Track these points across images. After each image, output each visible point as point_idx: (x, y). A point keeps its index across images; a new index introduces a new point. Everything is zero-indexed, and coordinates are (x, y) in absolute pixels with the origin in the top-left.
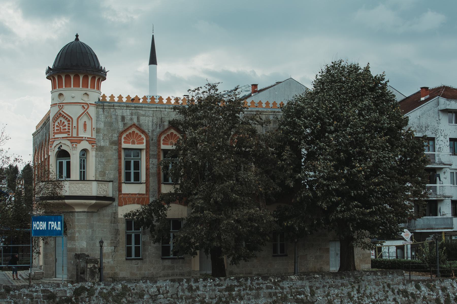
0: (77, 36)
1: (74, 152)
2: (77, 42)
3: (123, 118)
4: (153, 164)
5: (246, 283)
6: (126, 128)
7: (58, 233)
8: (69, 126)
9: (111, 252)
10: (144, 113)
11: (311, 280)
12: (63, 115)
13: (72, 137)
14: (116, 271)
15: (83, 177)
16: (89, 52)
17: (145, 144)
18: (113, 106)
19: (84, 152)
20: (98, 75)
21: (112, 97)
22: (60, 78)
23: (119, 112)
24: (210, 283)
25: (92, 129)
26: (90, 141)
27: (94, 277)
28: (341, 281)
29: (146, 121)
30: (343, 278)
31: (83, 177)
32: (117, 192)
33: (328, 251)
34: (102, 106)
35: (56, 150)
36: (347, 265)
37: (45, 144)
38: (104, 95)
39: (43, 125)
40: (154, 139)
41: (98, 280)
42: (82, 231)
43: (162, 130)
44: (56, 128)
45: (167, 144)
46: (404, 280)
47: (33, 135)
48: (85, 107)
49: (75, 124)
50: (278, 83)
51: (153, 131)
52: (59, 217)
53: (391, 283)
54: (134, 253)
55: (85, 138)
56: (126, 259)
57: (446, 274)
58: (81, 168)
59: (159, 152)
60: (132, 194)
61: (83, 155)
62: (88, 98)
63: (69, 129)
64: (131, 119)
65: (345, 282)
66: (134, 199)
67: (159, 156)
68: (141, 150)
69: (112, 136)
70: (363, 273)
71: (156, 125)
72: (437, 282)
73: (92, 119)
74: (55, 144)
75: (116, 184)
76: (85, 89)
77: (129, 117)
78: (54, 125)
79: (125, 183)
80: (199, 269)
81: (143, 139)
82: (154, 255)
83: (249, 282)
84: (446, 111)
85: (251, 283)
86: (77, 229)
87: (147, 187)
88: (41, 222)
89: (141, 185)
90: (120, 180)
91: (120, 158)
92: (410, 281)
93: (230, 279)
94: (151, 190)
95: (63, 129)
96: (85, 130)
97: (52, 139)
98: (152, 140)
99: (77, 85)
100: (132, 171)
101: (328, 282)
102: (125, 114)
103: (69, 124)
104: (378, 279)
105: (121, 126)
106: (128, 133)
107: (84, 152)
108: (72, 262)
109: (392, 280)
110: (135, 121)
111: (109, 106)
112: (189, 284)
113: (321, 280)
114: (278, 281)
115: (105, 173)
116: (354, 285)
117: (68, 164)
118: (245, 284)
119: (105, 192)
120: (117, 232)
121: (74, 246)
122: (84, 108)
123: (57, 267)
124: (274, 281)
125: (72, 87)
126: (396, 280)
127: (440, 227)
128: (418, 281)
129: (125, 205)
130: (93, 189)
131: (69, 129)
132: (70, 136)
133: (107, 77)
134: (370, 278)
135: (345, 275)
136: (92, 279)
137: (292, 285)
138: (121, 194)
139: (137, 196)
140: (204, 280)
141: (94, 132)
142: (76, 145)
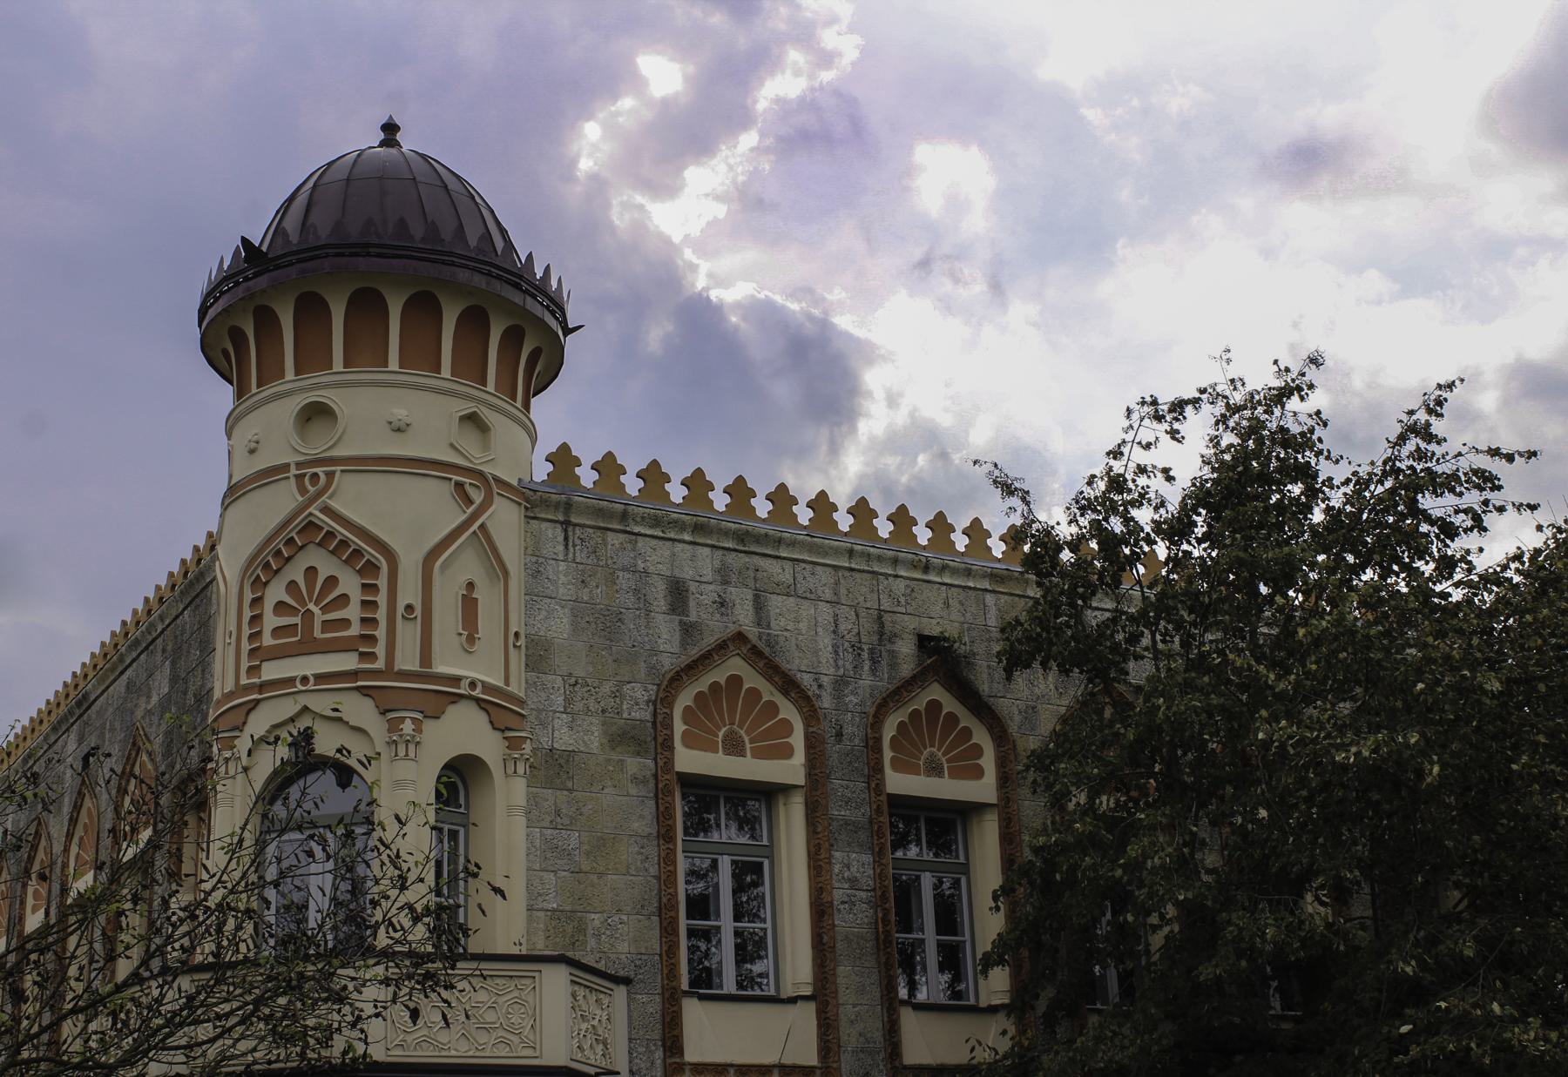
0: (390, 128)
1: (405, 770)
3: (678, 593)
4: (853, 882)
6: (695, 652)
8: (368, 605)
10: (787, 577)
12: (331, 534)
13: (389, 672)
17: (799, 757)
18: (624, 516)
19: (460, 777)
21: (608, 467)
22: (311, 310)
23: (657, 557)
25: (511, 640)
26: (498, 709)
29: (803, 626)
32: (659, 1054)
34: (557, 506)
38: (564, 448)
43: (885, 684)
44: (271, 621)
48: (471, 492)
49: (409, 592)
51: (840, 683)
55: (473, 685)
62: (486, 446)
63: (368, 622)
64: (722, 604)
71: (856, 648)
74: (259, 724)
75: (652, 1004)
77: (710, 593)
78: (257, 601)
79: (702, 998)
81: (787, 727)
89: (790, 1008)
90: (672, 973)
94: (849, 1035)
95: (327, 625)
99: (422, 355)
102: (687, 573)
106: (703, 684)
107: (460, 777)
110: (744, 616)
111: (600, 513)
115: (581, 930)
122: (470, 502)
125: (394, 364)
131: (372, 622)
132: (380, 664)
138: (681, 1067)
141: (517, 660)
142: (418, 730)
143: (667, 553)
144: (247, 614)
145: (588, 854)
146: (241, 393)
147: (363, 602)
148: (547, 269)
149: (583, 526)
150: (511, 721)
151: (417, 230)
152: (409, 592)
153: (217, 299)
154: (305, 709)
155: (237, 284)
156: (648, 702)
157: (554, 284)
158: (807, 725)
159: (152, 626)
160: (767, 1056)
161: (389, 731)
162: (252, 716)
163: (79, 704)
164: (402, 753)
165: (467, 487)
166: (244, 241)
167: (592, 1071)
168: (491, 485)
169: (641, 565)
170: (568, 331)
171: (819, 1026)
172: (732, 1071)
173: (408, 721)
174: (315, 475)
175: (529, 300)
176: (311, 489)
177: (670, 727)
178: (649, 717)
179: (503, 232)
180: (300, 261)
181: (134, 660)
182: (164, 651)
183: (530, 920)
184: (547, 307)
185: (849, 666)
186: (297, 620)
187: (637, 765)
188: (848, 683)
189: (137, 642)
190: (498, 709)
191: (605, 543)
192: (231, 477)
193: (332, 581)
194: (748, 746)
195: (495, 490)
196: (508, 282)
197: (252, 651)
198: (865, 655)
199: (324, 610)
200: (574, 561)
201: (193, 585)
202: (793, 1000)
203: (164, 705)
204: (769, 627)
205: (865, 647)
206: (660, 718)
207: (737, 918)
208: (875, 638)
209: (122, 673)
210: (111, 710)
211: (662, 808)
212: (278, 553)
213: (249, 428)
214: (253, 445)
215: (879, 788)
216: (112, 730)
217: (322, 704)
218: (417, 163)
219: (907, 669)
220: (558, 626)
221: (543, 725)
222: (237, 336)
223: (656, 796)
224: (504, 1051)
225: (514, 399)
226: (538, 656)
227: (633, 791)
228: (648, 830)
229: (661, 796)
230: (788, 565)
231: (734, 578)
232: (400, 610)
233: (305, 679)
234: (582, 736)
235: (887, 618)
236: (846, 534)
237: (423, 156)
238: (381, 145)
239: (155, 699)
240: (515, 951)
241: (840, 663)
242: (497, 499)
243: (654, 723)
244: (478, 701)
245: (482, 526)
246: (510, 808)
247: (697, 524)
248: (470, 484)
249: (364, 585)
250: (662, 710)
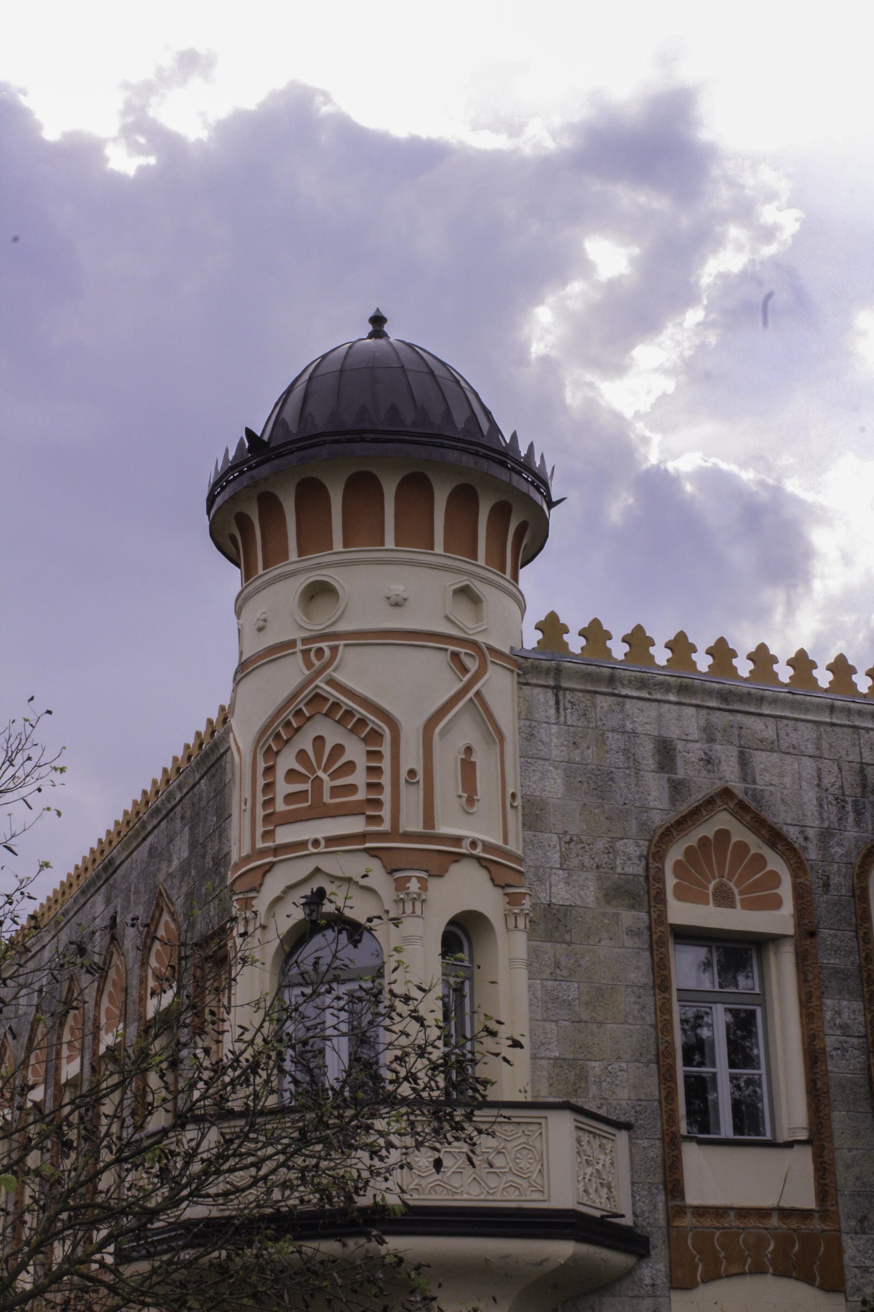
0: (378, 321)
3: (666, 753)
4: (845, 1029)
6: (684, 808)
12: (336, 705)
13: (394, 834)
17: (788, 908)
18: (612, 680)
21: (595, 633)
22: (311, 494)
23: (645, 718)
25: (508, 800)
29: (787, 780)
32: (661, 1198)
34: (548, 671)
35: (293, 914)
38: (553, 617)
40: (835, 880)
44: (283, 788)
48: (467, 661)
49: (411, 758)
51: (826, 835)
55: (474, 844)
60: (744, 1213)
62: (479, 618)
71: (840, 801)
74: (273, 886)
77: (695, 751)
78: (270, 770)
79: (701, 1142)
81: (774, 879)
87: (823, 1170)
89: (788, 1154)
90: (671, 1119)
95: (336, 791)
99: (416, 534)
102: (674, 733)
103: (374, 755)
106: (693, 838)
107: (462, 935)
110: (729, 773)
111: (588, 677)
115: (583, 1076)
122: (465, 670)
125: (390, 542)
129: (713, 1276)
130: (556, 1166)
132: (386, 827)
138: (682, 1210)
139: (774, 1221)
141: (515, 820)
142: (424, 888)
143: (654, 714)
144: (261, 782)
145: (587, 1004)
146: (248, 574)
147: (370, 769)
148: (531, 447)
149: (573, 690)
150: (511, 878)
151: (408, 416)
153: (223, 488)
154: (317, 870)
155: (242, 473)
156: (640, 857)
157: (538, 463)
159: (171, 795)
160: (764, 1198)
161: (397, 889)
162: (269, 879)
163: (105, 869)
164: (409, 910)
165: (463, 657)
166: (249, 433)
167: (598, 1214)
168: (485, 654)
169: (629, 726)
170: (551, 504)
171: (816, 1170)
172: (732, 1214)
173: (414, 880)
174: (320, 651)
175: (515, 477)
176: (317, 663)
177: (661, 880)
178: (640, 870)
179: (488, 413)
180: (299, 449)
181: (155, 827)
182: (183, 818)
183: (534, 1068)
184: (532, 483)
185: (834, 818)
186: (307, 786)
187: (632, 918)
188: (832, 835)
189: (157, 810)
190: (497, 866)
191: (594, 706)
192: (241, 654)
193: (338, 749)
194: (738, 898)
195: (489, 658)
196: (494, 460)
197: (267, 818)
198: (849, 807)
199: (333, 776)
200: (565, 723)
201: (208, 756)
202: (789, 1145)
203: (184, 870)
204: (754, 782)
205: (849, 800)
206: (652, 872)
207: (732, 1064)
208: (858, 790)
209: (144, 839)
210: (134, 873)
211: (656, 959)
212: (288, 724)
213: (257, 608)
214: (261, 623)
216: (137, 892)
217: (332, 865)
218: (404, 351)
220: (553, 786)
221: (541, 880)
222: (243, 522)
223: (651, 948)
224: (513, 1195)
225: (503, 570)
226: (534, 814)
227: (629, 942)
228: (644, 980)
230: (771, 722)
231: (719, 736)
232: (403, 774)
233: (316, 843)
236: (826, 691)
237: (410, 346)
238: (371, 336)
239: (175, 863)
240: (521, 1098)
241: (825, 815)
242: (491, 668)
243: (647, 877)
244: (479, 859)
245: (478, 694)
246: (512, 961)
247: (681, 684)
248: (465, 654)
249: (369, 753)
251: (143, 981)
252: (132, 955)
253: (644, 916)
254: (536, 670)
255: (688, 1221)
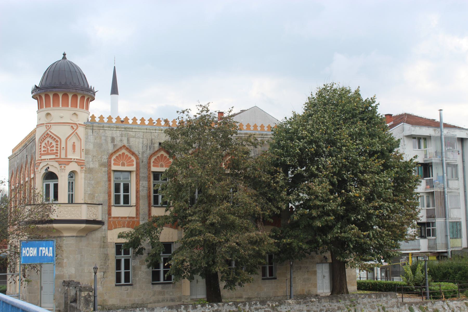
0: (64, 54)
1: (63, 174)
2: (65, 61)
3: (113, 139)
4: (144, 187)
5: (244, 308)
6: (116, 149)
7: (49, 260)
8: (57, 147)
9: (101, 278)
10: (134, 135)
11: (308, 304)
12: (51, 136)
13: (60, 158)
14: (106, 297)
15: (71, 200)
16: (77, 71)
17: (135, 166)
18: (103, 127)
20: (87, 95)
21: (101, 118)
22: (47, 96)
23: (109, 133)
24: (209, 309)
25: (81, 150)
26: (79, 163)
27: (89, 305)
28: (337, 304)
30: (339, 302)
31: (71, 200)
32: (107, 216)
33: (315, 273)
35: (43, 171)
36: (338, 287)
37: (26, 167)
38: (93, 115)
39: (23, 147)
40: (144, 161)
41: (92, 309)
42: (71, 256)
43: (152, 152)
44: (43, 149)
45: (157, 166)
46: (397, 302)
47: (9, 158)
49: (63, 145)
50: (242, 111)
51: (143, 153)
52: (51, 242)
53: (385, 305)
54: (123, 278)
55: (74, 159)
56: (116, 285)
57: (436, 296)
58: (69, 191)
59: (149, 174)
60: (122, 218)
61: (72, 177)
63: (57, 150)
65: (341, 305)
66: (124, 223)
67: (149, 178)
68: (130, 172)
69: (101, 158)
70: (358, 296)
71: (147, 146)
72: (429, 304)
73: (81, 140)
74: (41, 165)
75: (106, 208)
76: (74, 109)
77: (119, 139)
78: (40, 146)
79: (115, 206)
80: (189, 294)
81: (133, 161)
82: (144, 280)
83: (247, 307)
84: (412, 137)
85: (250, 308)
86: (65, 255)
87: (137, 210)
88: (31, 248)
90: (110, 203)
91: (109, 180)
92: (403, 304)
93: (228, 305)
94: (141, 212)
95: (51, 150)
96: (74, 152)
97: (38, 160)
98: (142, 162)
99: (65, 104)
100: (122, 194)
101: (325, 306)
102: (115, 136)
104: (373, 302)
105: (111, 148)
107: (72, 174)
108: (60, 290)
109: (387, 303)
111: (99, 127)
112: (187, 310)
113: (318, 304)
114: (276, 306)
115: (94, 196)
116: (350, 308)
117: (56, 186)
118: (244, 310)
119: (94, 216)
120: (106, 257)
121: (62, 273)
122: (73, 129)
123: (42, 295)
124: (272, 305)
125: (61, 106)
126: (390, 303)
127: (408, 248)
128: (411, 304)
130: (84, 213)
131: (57, 150)
132: (59, 157)
133: (95, 97)
134: (365, 301)
135: (340, 298)
136: (87, 308)
137: (290, 309)
139: (127, 219)
140: (202, 306)
141: (83, 154)
142: (65, 167)
152: (63, 145)
158: (136, 160)
177: (110, 162)
178: (107, 161)
186: (46, 149)
189: (31, 139)
193: (51, 143)
199: (51, 148)
202: (132, 206)
215: (149, 170)
219: (156, 149)
220: (91, 147)
221: (88, 164)
226: (87, 152)
229: (109, 174)
232: (62, 147)
234: (95, 165)
235: (153, 140)
238: (63, 58)
250: (109, 160)
251: (30, 171)
252: (29, 165)
253: (107, 169)
254: (89, 126)
255: (112, 219)
